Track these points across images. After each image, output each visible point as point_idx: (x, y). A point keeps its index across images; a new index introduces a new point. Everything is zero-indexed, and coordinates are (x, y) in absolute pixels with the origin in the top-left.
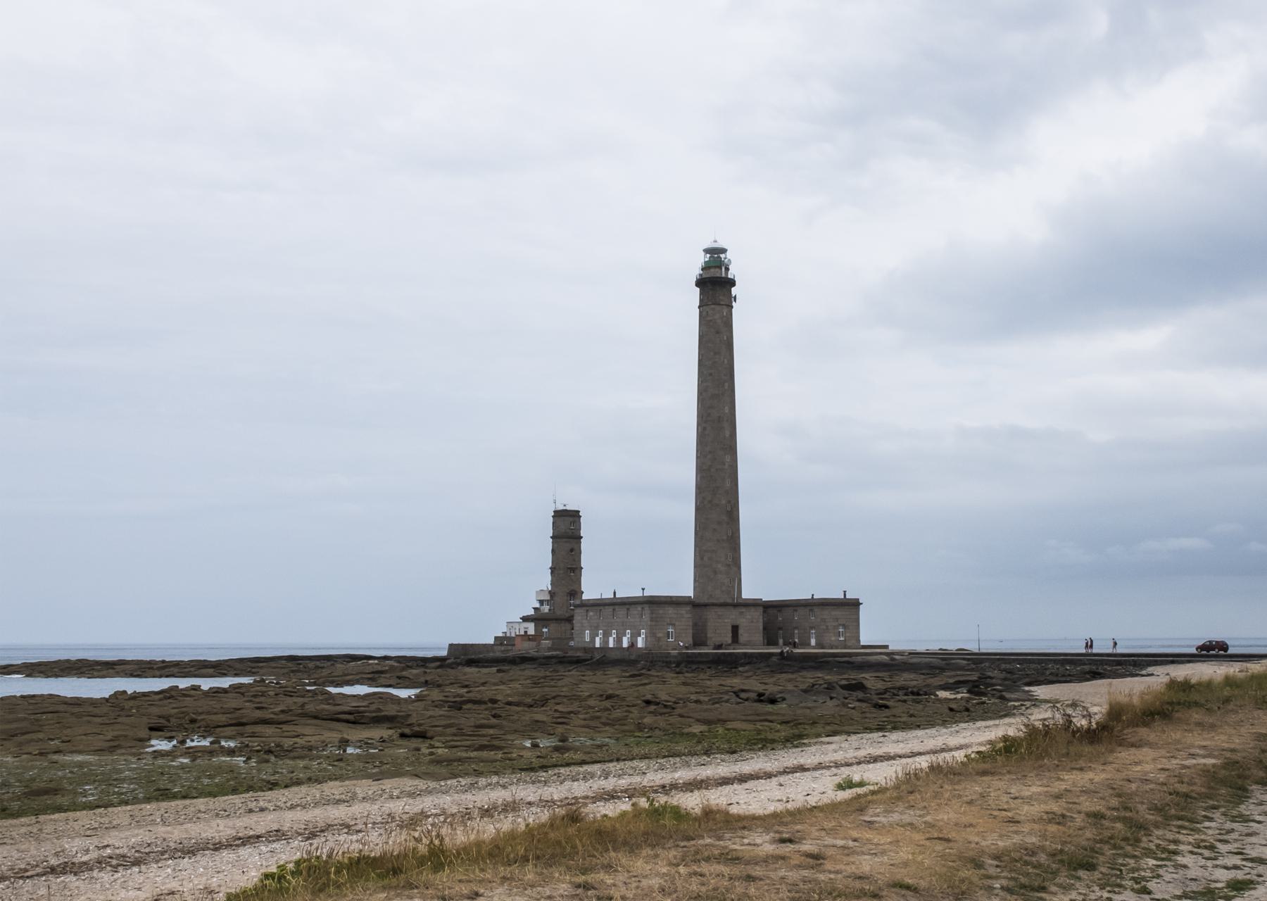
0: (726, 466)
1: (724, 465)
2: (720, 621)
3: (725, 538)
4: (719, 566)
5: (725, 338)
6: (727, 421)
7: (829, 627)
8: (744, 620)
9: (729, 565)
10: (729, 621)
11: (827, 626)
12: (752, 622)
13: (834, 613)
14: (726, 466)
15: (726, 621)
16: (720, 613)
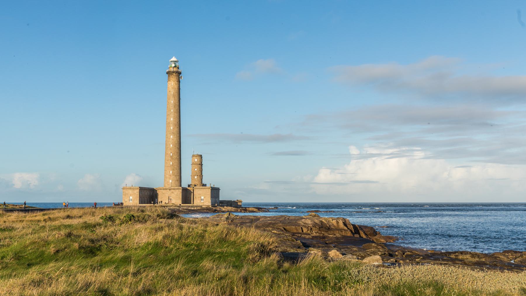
0: (171, 140)
1: (170, 139)
2: (163, 195)
3: (169, 165)
4: (167, 175)
5: (172, 93)
6: (172, 123)
7: (197, 197)
8: (174, 195)
9: (170, 175)
10: (168, 195)
11: (196, 197)
12: (177, 195)
13: (198, 192)
14: (171, 140)
15: (166, 195)
16: (164, 192)
